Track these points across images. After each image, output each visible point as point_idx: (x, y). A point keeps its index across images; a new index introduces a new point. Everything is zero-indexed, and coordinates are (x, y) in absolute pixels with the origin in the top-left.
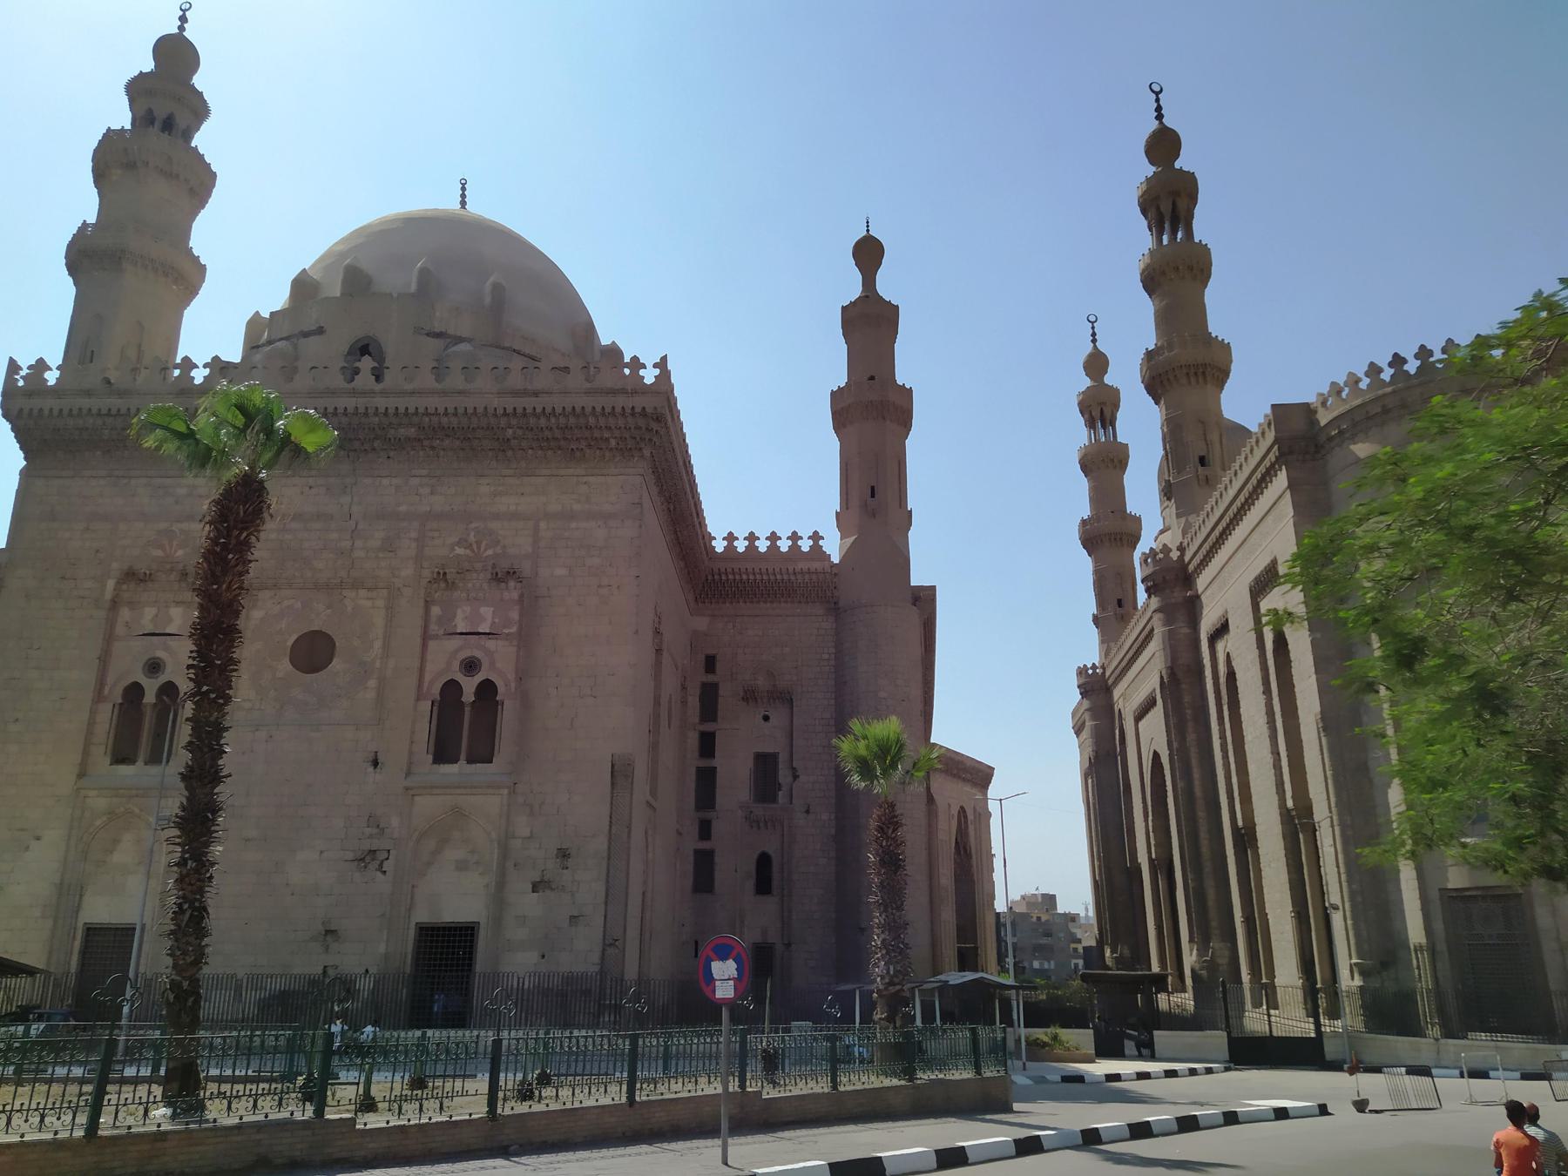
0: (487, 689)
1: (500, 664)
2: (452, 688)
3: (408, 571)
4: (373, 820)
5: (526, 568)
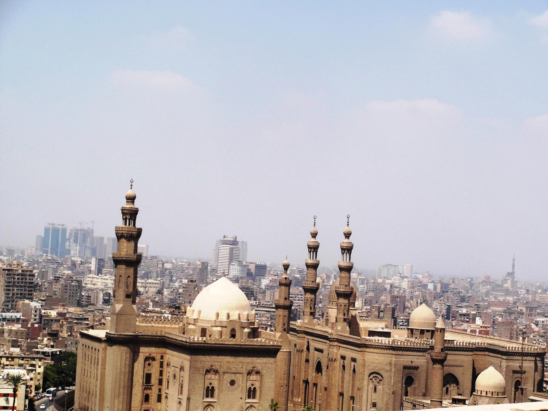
0: (255, 388)
1: (257, 385)
2: (250, 388)
3: (245, 371)
4: (242, 407)
5: (261, 371)
